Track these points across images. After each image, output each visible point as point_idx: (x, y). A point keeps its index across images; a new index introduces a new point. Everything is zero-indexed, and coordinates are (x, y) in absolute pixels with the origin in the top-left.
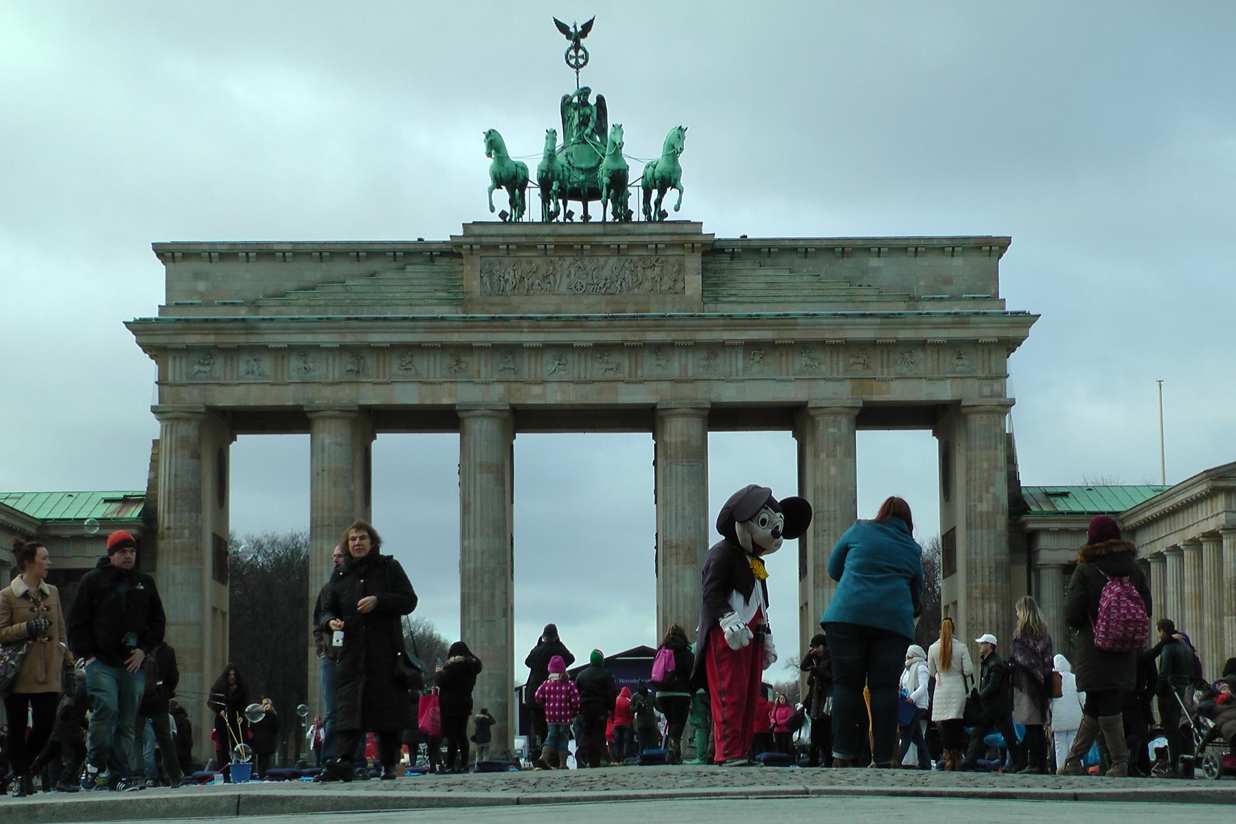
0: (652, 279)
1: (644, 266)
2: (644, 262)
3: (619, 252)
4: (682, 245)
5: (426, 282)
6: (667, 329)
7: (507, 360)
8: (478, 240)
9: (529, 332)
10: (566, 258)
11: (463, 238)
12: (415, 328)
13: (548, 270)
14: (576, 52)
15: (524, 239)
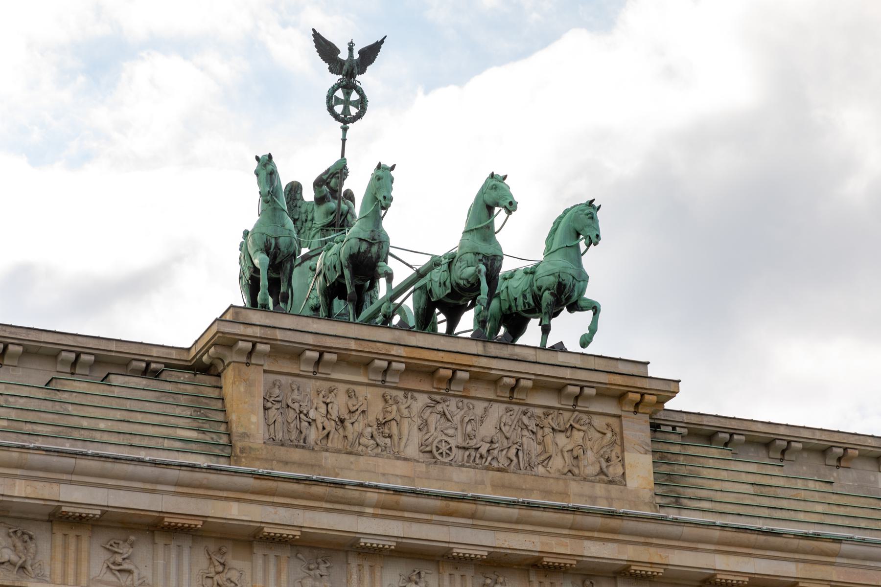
0: (567, 451)
1: (554, 426)
2: (553, 418)
3: (511, 397)
4: (620, 397)
5: (154, 408)
6: (621, 537)
7: (318, 572)
8: (269, 333)
9: (375, 516)
10: (416, 395)
11: (242, 326)
12: (157, 482)
13: (385, 411)
14: (348, 94)
15: (353, 345)
